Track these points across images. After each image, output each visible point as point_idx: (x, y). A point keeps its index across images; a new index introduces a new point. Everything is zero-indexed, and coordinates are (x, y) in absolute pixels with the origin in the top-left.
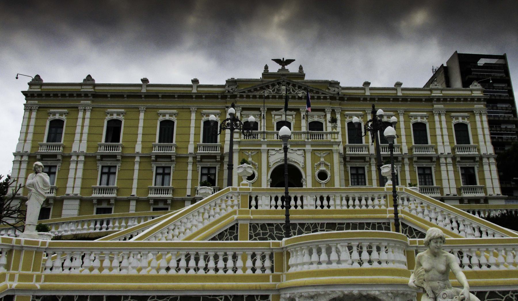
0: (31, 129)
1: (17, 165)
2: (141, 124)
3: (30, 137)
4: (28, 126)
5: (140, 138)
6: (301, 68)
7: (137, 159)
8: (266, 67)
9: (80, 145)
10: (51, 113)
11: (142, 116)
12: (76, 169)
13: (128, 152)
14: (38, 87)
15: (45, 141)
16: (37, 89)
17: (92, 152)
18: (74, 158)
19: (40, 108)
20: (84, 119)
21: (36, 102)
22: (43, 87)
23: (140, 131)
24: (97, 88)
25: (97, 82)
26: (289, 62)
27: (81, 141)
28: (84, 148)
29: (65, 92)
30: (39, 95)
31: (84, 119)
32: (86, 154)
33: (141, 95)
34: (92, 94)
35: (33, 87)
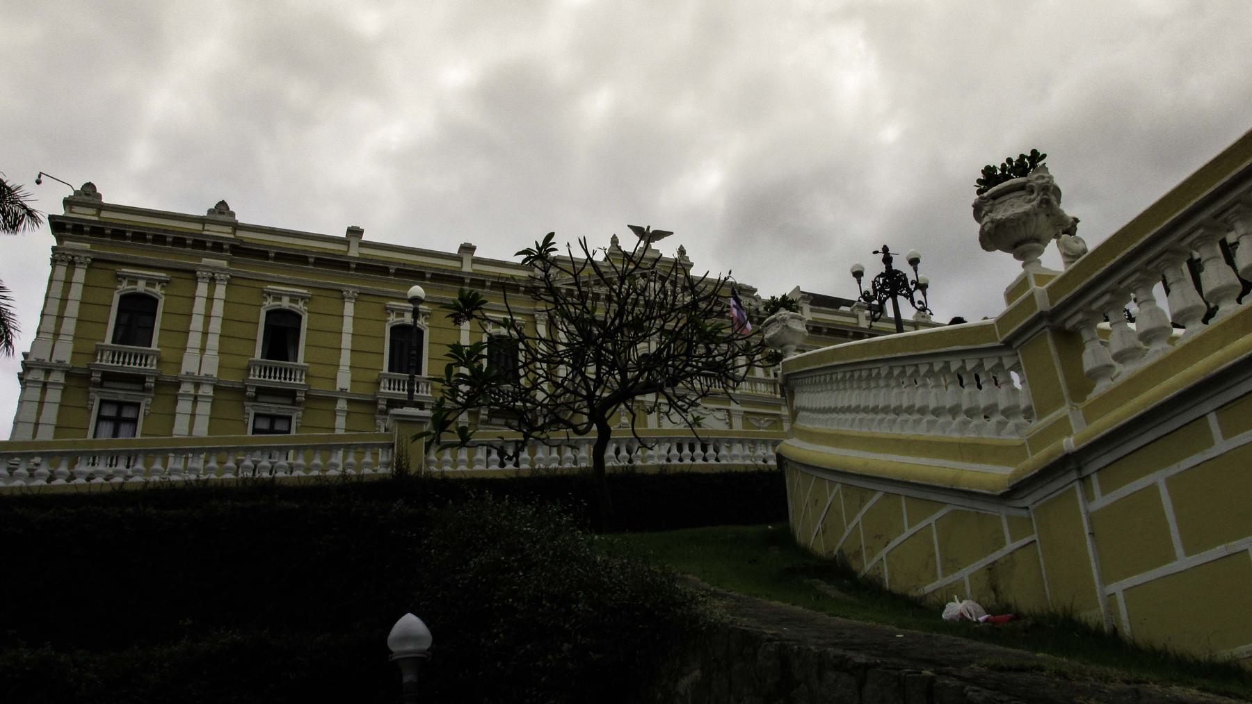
0: (73, 309)
1: (35, 393)
2: (348, 326)
3: (69, 326)
4: (64, 300)
5: (346, 358)
6: (682, 251)
7: (342, 405)
8: (614, 240)
9: (202, 357)
10: (124, 277)
11: (349, 308)
12: (193, 415)
13: (320, 387)
14: (93, 211)
15: (108, 341)
16: (87, 214)
17: (233, 379)
18: (187, 388)
19: (97, 262)
20: (210, 299)
21: (88, 246)
22: (104, 214)
23: (347, 342)
24: (240, 234)
25: (241, 218)
26: (660, 235)
27: (203, 350)
28: (211, 366)
29: (165, 231)
30: (97, 231)
31: (210, 299)
32: (219, 381)
33: (348, 263)
34: (232, 246)
35: (76, 209)
